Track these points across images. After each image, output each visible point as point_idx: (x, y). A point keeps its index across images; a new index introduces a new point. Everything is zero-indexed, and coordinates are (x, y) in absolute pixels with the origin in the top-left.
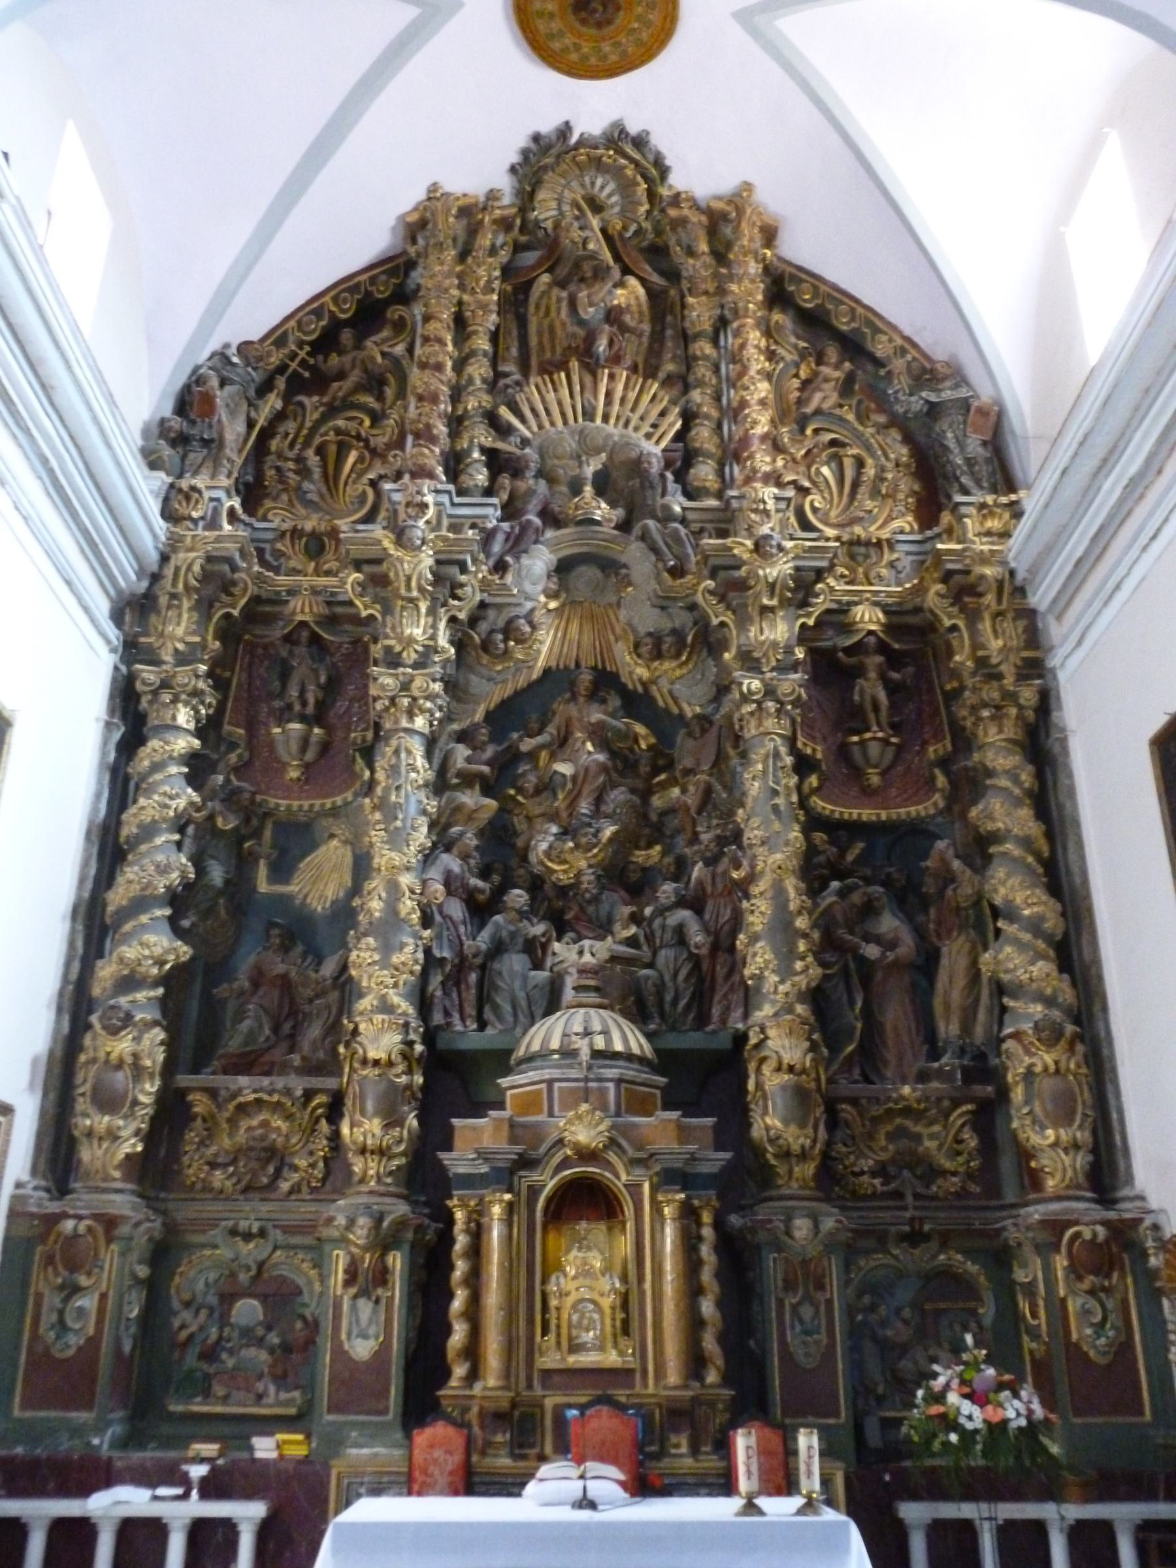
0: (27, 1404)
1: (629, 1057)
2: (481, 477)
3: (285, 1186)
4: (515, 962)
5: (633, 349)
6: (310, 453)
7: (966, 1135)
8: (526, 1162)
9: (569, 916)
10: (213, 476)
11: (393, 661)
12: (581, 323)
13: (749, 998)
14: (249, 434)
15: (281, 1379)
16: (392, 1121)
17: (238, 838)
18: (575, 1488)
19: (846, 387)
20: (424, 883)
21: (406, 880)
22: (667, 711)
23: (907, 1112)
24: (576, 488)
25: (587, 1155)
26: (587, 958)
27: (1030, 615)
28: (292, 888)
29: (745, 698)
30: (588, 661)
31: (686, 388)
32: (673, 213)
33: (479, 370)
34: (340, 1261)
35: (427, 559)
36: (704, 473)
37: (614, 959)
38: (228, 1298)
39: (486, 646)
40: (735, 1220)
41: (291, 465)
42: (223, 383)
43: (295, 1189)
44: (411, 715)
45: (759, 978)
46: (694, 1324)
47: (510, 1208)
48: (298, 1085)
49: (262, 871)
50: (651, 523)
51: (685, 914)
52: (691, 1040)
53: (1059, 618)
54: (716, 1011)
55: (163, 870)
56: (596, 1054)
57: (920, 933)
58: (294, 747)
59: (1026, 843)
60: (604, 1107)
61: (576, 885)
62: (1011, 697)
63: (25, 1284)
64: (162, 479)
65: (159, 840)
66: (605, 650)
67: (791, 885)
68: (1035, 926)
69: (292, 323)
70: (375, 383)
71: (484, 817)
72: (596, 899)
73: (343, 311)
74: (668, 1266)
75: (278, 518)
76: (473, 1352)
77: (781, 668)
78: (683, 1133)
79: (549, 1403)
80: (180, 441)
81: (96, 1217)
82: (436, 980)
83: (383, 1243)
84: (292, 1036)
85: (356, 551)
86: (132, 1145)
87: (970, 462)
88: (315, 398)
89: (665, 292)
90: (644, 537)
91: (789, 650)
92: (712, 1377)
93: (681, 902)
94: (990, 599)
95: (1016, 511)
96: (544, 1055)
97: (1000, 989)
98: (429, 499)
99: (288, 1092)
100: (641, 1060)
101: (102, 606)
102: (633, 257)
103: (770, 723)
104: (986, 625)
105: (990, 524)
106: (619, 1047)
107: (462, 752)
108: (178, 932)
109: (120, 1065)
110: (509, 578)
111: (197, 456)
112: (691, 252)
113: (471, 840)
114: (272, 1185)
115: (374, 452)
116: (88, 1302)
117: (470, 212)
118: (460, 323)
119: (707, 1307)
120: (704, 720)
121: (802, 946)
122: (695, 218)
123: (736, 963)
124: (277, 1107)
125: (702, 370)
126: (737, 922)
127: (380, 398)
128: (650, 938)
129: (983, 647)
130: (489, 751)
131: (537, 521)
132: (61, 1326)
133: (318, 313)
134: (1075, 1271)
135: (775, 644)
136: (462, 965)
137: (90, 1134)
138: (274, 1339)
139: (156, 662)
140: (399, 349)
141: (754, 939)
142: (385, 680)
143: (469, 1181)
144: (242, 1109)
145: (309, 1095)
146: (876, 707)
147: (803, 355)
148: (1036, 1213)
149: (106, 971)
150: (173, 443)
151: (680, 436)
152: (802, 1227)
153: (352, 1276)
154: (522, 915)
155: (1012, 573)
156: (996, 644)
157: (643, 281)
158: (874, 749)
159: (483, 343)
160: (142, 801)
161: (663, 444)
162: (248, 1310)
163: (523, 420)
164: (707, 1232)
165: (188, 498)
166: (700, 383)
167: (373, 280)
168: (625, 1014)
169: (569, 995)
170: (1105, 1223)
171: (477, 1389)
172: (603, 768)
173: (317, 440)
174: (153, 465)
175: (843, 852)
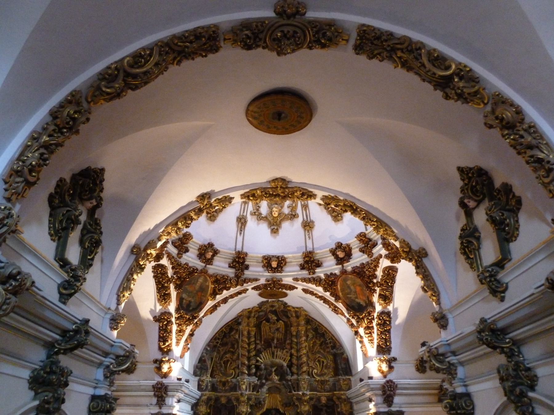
6: (222, 362)
10: (206, 375)
14: (212, 363)
19: (321, 345)
30: (274, 407)
31: (292, 348)
32: (288, 308)
33: (253, 346)
35: (246, 397)
36: (294, 369)
41: (218, 365)
42: (207, 354)
50: (284, 382)
64: (197, 378)
73: (227, 331)
87: (342, 368)
88: (222, 348)
89: (287, 322)
90: (283, 384)
104: (343, 405)
105: (345, 383)
111: (203, 371)
112: (292, 316)
118: (249, 333)
122: (292, 310)
127: (234, 348)
129: (342, 409)
131: (264, 381)
133: (222, 331)
135: (306, 411)
140: (237, 337)
147: (313, 335)
151: (290, 360)
155: (347, 397)
156: (344, 409)
159: (253, 339)
161: (287, 362)
163: (261, 359)
166: (293, 348)
167: (232, 323)
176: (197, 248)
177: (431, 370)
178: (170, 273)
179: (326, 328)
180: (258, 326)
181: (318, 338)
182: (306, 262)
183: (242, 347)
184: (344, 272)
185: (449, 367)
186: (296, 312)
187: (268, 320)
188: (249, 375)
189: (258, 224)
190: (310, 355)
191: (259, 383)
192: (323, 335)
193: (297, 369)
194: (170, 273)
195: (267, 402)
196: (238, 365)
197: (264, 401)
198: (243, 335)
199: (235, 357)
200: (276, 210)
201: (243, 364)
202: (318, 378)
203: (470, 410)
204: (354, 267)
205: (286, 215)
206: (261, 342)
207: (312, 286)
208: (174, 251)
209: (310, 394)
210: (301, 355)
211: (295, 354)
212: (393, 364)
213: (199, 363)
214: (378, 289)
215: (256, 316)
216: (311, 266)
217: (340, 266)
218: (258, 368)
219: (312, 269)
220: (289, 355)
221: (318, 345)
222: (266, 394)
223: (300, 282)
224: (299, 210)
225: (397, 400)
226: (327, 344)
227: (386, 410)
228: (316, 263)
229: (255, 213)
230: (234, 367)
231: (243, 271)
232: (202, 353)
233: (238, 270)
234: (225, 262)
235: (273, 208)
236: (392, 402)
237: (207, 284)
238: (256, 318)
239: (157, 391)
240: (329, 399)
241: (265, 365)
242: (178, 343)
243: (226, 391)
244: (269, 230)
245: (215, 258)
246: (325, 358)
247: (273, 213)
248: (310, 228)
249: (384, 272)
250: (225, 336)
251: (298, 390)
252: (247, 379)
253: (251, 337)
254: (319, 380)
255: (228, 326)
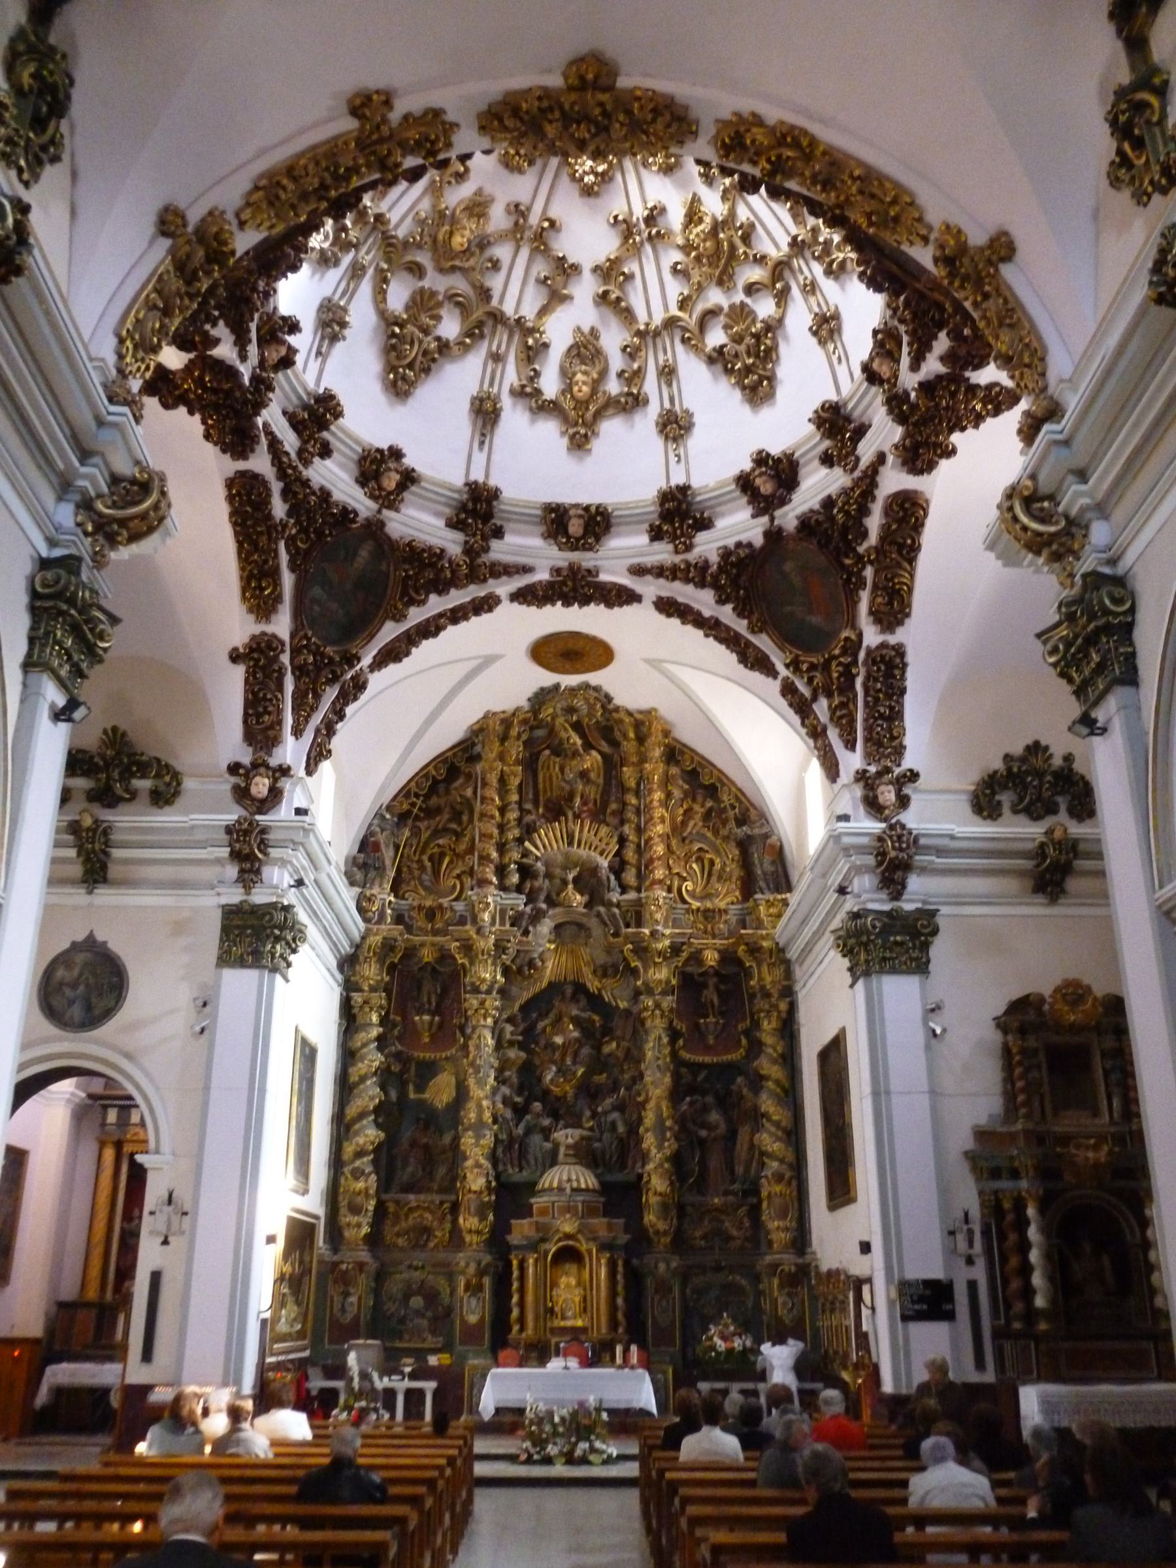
0: (330, 1342)
1: (587, 1190)
2: (515, 879)
3: (431, 1245)
4: (536, 1139)
5: (593, 793)
6: (425, 858)
7: (746, 1220)
8: (543, 1240)
9: (562, 1112)
11: (476, 990)
12: (567, 782)
13: (645, 1157)
15: (434, 1332)
16: (483, 1218)
17: (402, 1073)
18: (563, 1364)
19: (707, 816)
20: (494, 1103)
21: (485, 1103)
22: (609, 1004)
23: (717, 1209)
24: (565, 883)
25: (568, 1236)
26: (570, 1141)
27: (787, 963)
28: (426, 1096)
29: (646, 1009)
30: (570, 978)
31: (622, 822)
32: (615, 715)
33: (513, 815)
34: (462, 1282)
36: (630, 877)
37: (582, 1138)
38: (407, 1297)
39: (520, 971)
40: (635, 1262)
41: (415, 866)
42: (382, 830)
43: (436, 1246)
44: (485, 1018)
45: (649, 1150)
46: (613, 1308)
47: (536, 1260)
48: (437, 1198)
49: (411, 1087)
50: (602, 909)
51: (615, 1115)
52: (618, 1177)
53: (801, 964)
54: (630, 1163)
55: (372, 1098)
56: (573, 1190)
57: (729, 1121)
58: (426, 1026)
59: (777, 1082)
60: (576, 1214)
61: (565, 1097)
62: (776, 1007)
63: (325, 1293)
64: (358, 890)
65: (369, 1082)
66: (579, 971)
67: (664, 1105)
68: (777, 1124)
69: (413, 784)
70: (456, 816)
71: (520, 1062)
72: (574, 1105)
74: (603, 1284)
75: (412, 900)
76: (522, 1320)
77: (664, 993)
78: (610, 1227)
79: (554, 1340)
80: (364, 867)
81: (355, 1262)
82: (500, 1151)
83: (481, 1273)
84: (431, 1173)
85: (456, 935)
86: (366, 1230)
90: (599, 915)
91: (668, 982)
92: (621, 1330)
93: (615, 1108)
94: (767, 956)
95: (785, 903)
96: (551, 1189)
97: (763, 1154)
98: (490, 900)
99: (432, 1202)
100: (594, 1191)
101: (333, 963)
102: (594, 737)
103: (658, 1021)
104: (765, 968)
106: (583, 1186)
107: (509, 1028)
108: (378, 1126)
109: (359, 1193)
110: (530, 937)
111: (372, 874)
112: (625, 736)
113: (515, 1080)
114: (425, 1245)
115: (458, 856)
116: (353, 1299)
117: (507, 721)
118: (502, 780)
119: (620, 1301)
120: (627, 1013)
121: (668, 1134)
122: (627, 719)
123: (639, 1140)
124: (428, 1209)
125: (630, 815)
126: (640, 1120)
127: (460, 823)
128: (599, 1125)
130: (521, 1028)
131: (544, 906)
132: (343, 1310)
133: (426, 776)
134: (781, 1286)
135: (660, 981)
136: (512, 1139)
137: (349, 1225)
138: (429, 1314)
139: (360, 990)
140: (469, 792)
141: (647, 1130)
142: (473, 1002)
143: (518, 1247)
144: (411, 1210)
145: (442, 1203)
146: (713, 1005)
147: (686, 794)
148: (768, 1259)
149: (349, 1149)
150: (359, 868)
151: (618, 854)
152: (662, 1267)
153: (467, 1289)
154: (538, 1115)
156: (768, 979)
157: (600, 752)
158: (711, 1027)
159: (515, 797)
160: (360, 1065)
162: (417, 1302)
163: (537, 847)
164: (620, 1269)
165: (369, 900)
166: (629, 821)
167: (455, 755)
168: (588, 1166)
169: (561, 1157)
170: (796, 1265)
171: (524, 1335)
172: (577, 1040)
173: (429, 852)
174: (352, 883)
175: (695, 1076)
176: (356, 457)
177: (1015, 811)
178: (279, 509)
179: (720, 771)
180: (531, 764)
181: (700, 798)
182: (667, 515)
183: (483, 815)
184: (774, 535)
185: (1067, 532)
186: (638, 725)
187: (558, 751)
188: (503, 887)
189: (533, 421)
190: (674, 842)
191: (528, 909)
192: (712, 791)
193: (639, 876)
194: (279, 509)
195: (549, 964)
196: (472, 868)
197: (543, 961)
198: (485, 784)
199: (462, 847)
200: (584, 378)
201: (484, 859)
202: (696, 904)
203: (1124, 613)
204: (804, 514)
205: (610, 398)
206: (537, 807)
207: (684, 592)
208: (290, 441)
209: (672, 936)
210: (650, 838)
211: (632, 837)
212: (907, 790)
213: (360, 851)
214: (869, 572)
215: (524, 737)
216: (681, 527)
217: (765, 519)
218: (526, 872)
219: (682, 535)
220: (615, 839)
221: (698, 817)
222: (550, 942)
223: (649, 578)
224: (651, 385)
225: (915, 884)
226: (724, 810)
227: (886, 907)
228: (694, 518)
229: (523, 387)
230: (458, 871)
231: (485, 538)
232: (370, 825)
233: (474, 535)
234: (437, 514)
235: (574, 374)
236: (904, 887)
237: (384, 567)
238: (525, 743)
239: (238, 841)
240: (728, 957)
241: (547, 864)
242: (297, 732)
243: (435, 933)
244: (565, 441)
245: (406, 494)
246: (718, 852)
247: (576, 389)
248: (680, 428)
249: (887, 511)
250: (433, 790)
251: (639, 924)
252: (493, 897)
253: (507, 791)
254: (698, 910)
255: (445, 761)
